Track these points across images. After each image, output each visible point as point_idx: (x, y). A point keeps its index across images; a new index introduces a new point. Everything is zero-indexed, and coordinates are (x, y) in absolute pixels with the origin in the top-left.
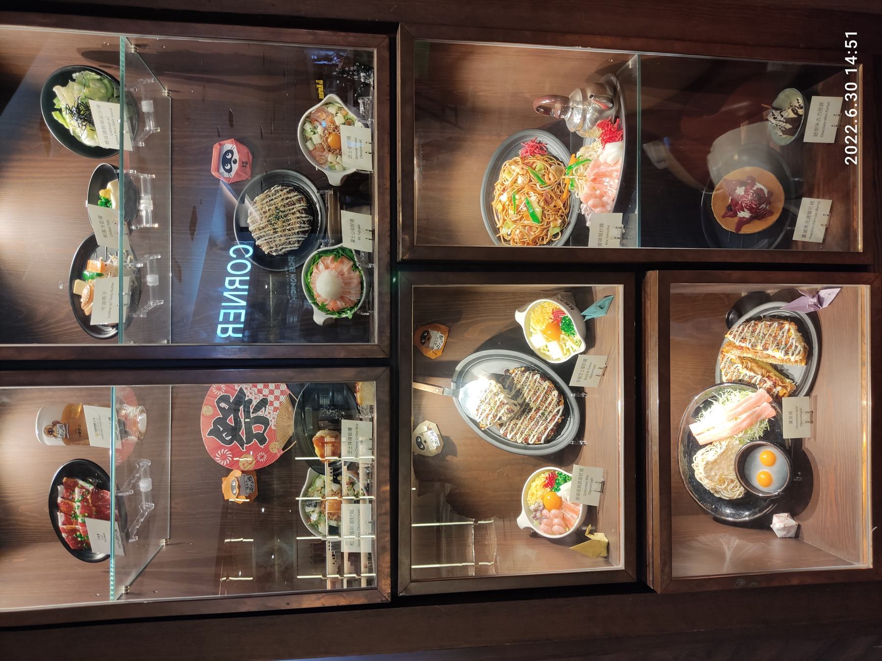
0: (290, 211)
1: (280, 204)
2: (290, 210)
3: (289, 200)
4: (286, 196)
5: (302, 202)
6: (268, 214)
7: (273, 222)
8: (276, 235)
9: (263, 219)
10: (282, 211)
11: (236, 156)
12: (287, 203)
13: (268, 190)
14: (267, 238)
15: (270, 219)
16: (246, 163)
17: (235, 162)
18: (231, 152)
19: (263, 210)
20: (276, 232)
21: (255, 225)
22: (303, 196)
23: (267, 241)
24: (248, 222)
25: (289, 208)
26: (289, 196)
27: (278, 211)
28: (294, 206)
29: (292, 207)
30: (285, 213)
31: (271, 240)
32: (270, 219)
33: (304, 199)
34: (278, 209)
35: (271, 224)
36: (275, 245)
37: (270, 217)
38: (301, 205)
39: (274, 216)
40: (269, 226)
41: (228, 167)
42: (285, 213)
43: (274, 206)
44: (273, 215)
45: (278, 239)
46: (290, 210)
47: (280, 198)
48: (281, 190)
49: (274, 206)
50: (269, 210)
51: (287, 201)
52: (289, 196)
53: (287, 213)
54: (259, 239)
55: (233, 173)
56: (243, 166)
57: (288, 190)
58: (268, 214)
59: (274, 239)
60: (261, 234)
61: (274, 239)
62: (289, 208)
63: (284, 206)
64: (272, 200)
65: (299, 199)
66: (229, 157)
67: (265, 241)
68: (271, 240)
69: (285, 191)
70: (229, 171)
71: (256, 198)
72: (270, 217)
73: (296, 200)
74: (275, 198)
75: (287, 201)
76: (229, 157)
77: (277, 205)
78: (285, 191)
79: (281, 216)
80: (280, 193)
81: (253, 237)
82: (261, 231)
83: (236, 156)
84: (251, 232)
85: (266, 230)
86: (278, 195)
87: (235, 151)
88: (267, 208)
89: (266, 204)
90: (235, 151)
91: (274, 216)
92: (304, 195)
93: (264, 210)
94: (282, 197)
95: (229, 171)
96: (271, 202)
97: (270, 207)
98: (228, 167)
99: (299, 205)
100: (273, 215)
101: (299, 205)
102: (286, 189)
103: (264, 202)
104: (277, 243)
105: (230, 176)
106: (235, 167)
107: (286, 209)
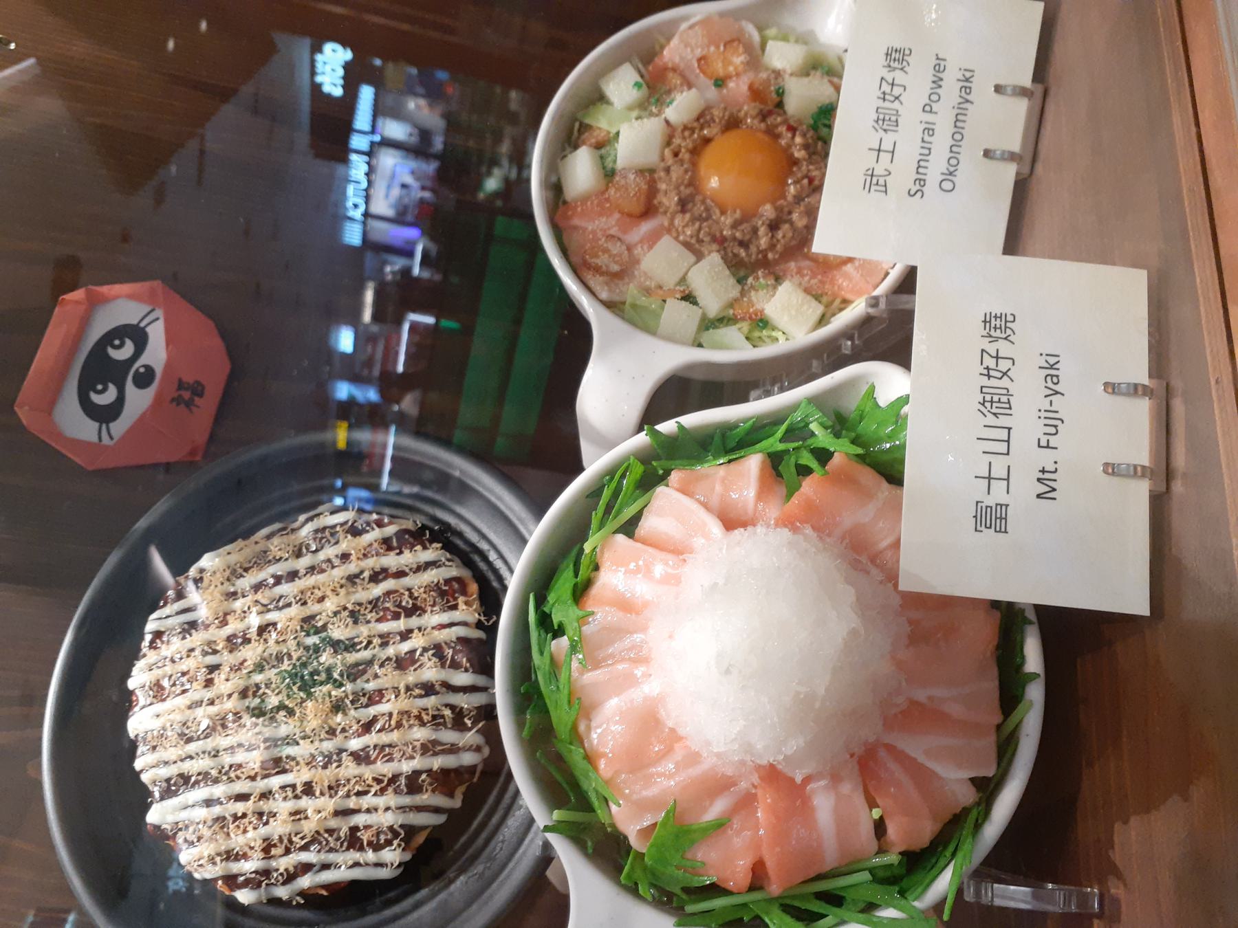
0: (384, 645)
1: (330, 605)
2: (385, 640)
3: (389, 584)
4: (372, 563)
5: (461, 600)
6: (251, 653)
7: (273, 701)
8: (276, 782)
9: (219, 677)
10: (336, 646)
11: (156, 354)
12: (375, 604)
13: (277, 526)
14: (219, 791)
15: (258, 678)
16: (198, 390)
17: (145, 379)
18: (138, 336)
19: (228, 630)
20: (278, 765)
21: (168, 704)
22: (465, 573)
23: (217, 810)
24: (132, 684)
25: (384, 627)
26: (391, 561)
27: (313, 640)
28: (414, 622)
29: (401, 624)
30: (352, 658)
31: (240, 807)
32: (258, 678)
33: (474, 588)
34: (317, 631)
35: (258, 712)
36: (258, 844)
37: (260, 668)
38: (456, 616)
39: (286, 665)
40: (248, 720)
41: (107, 397)
42: (352, 658)
43: (295, 611)
44: (279, 658)
45: (282, 807)
46: (385, 640)
47: (339, 573)
48: (355, 532)
49: (295, 611)
50: (262, 630)
51: (378, 590)
52: (391, 561)
53: (365, 654)
54: (169, 791)
55: (119, 427)
56: (178, 400)
57: (391, 530)
58: (251, 653)
59: (265, 806)
60: (191, 767)
61: (265, 806)
62: (384, 627)
63: (353, 614)
64: (293, 575)
65: (447, 581)
66: (124, 352)
67: (202, 813)
68: (240, 807)
69: (374, 535)
70: (106, 415)
71: (208, 561)
72: (260, 668)
73: (428, 588)
74: (312, 570)
75: (378, 590)
76: (124, 352)
77: (313, 608)
78: (374, 535)
79: (329, 671)
80: (346, 544)
81: (137, 775)
82: (192, 747)
83: (156, 354)
84: (133, 745)
85: (221, 741)
86: (330, 552)
87: (157, 333)
88: (254, 621)
89: (249, 599)
90: (157, 333)
91: (286, 665)
92: (468, 563)
93: (233, 626)
94: (352, 568)
95: (106, 415)
96: (285, 588)
97: (272, 616)
98: (107, 397)
99: (445, 618)
100: (279, 658)
101: (445, 618)
102: (380, 524)
103: (245, 583)
104: (278, 828)
105: (106, 440)
106: (138, 400)
107: (364, 631)
